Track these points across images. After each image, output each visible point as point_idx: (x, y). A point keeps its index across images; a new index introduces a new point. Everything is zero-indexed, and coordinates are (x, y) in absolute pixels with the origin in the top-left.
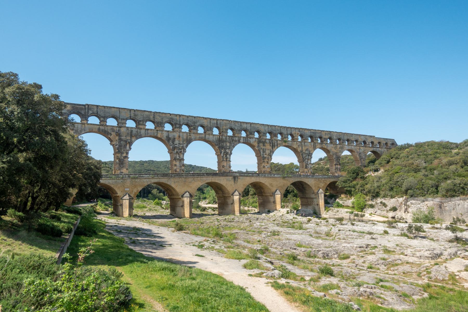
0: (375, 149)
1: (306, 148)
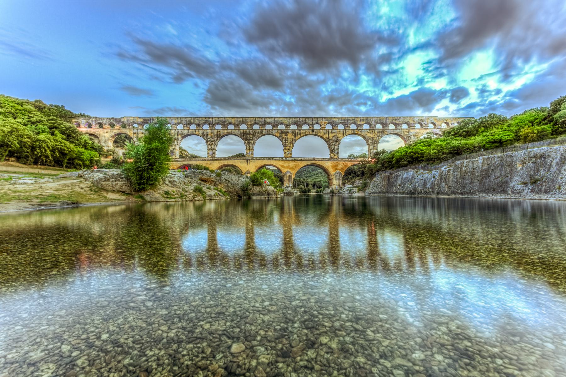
1: (333, 135)
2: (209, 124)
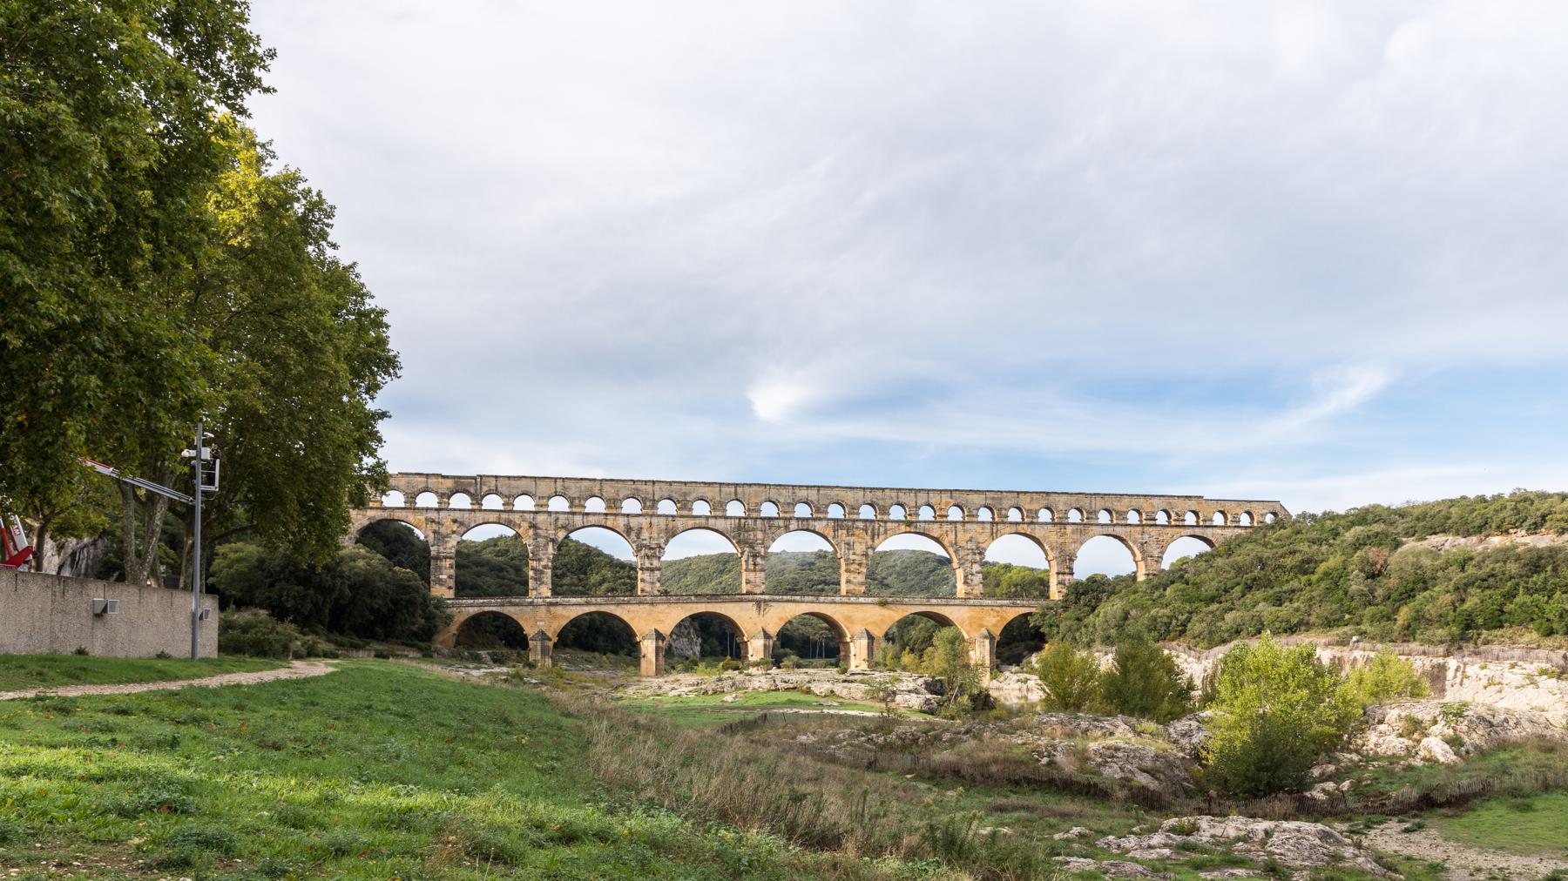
0: (1198, 531)
2: (643, 501)
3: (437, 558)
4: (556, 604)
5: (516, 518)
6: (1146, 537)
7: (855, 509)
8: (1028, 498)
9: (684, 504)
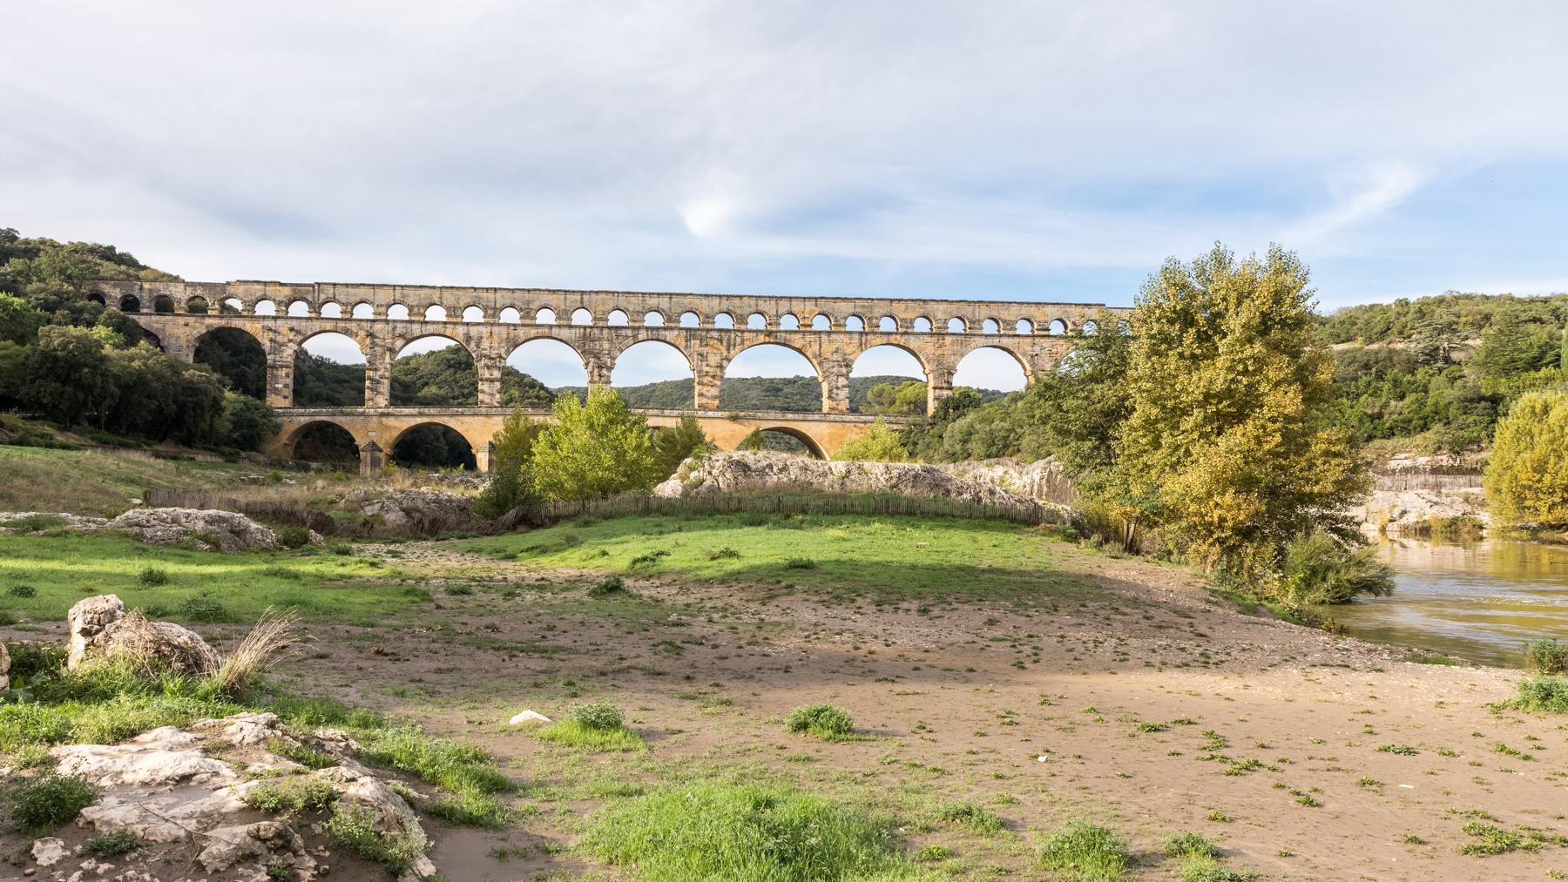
1: (834, 347)
2: (485, 309)
3: (273, 367)
4: (388, 415)
5: (353, 326)
6: (1037, 349)
7: (709, 318)
8: (902, 306)
9: (527, 313)
